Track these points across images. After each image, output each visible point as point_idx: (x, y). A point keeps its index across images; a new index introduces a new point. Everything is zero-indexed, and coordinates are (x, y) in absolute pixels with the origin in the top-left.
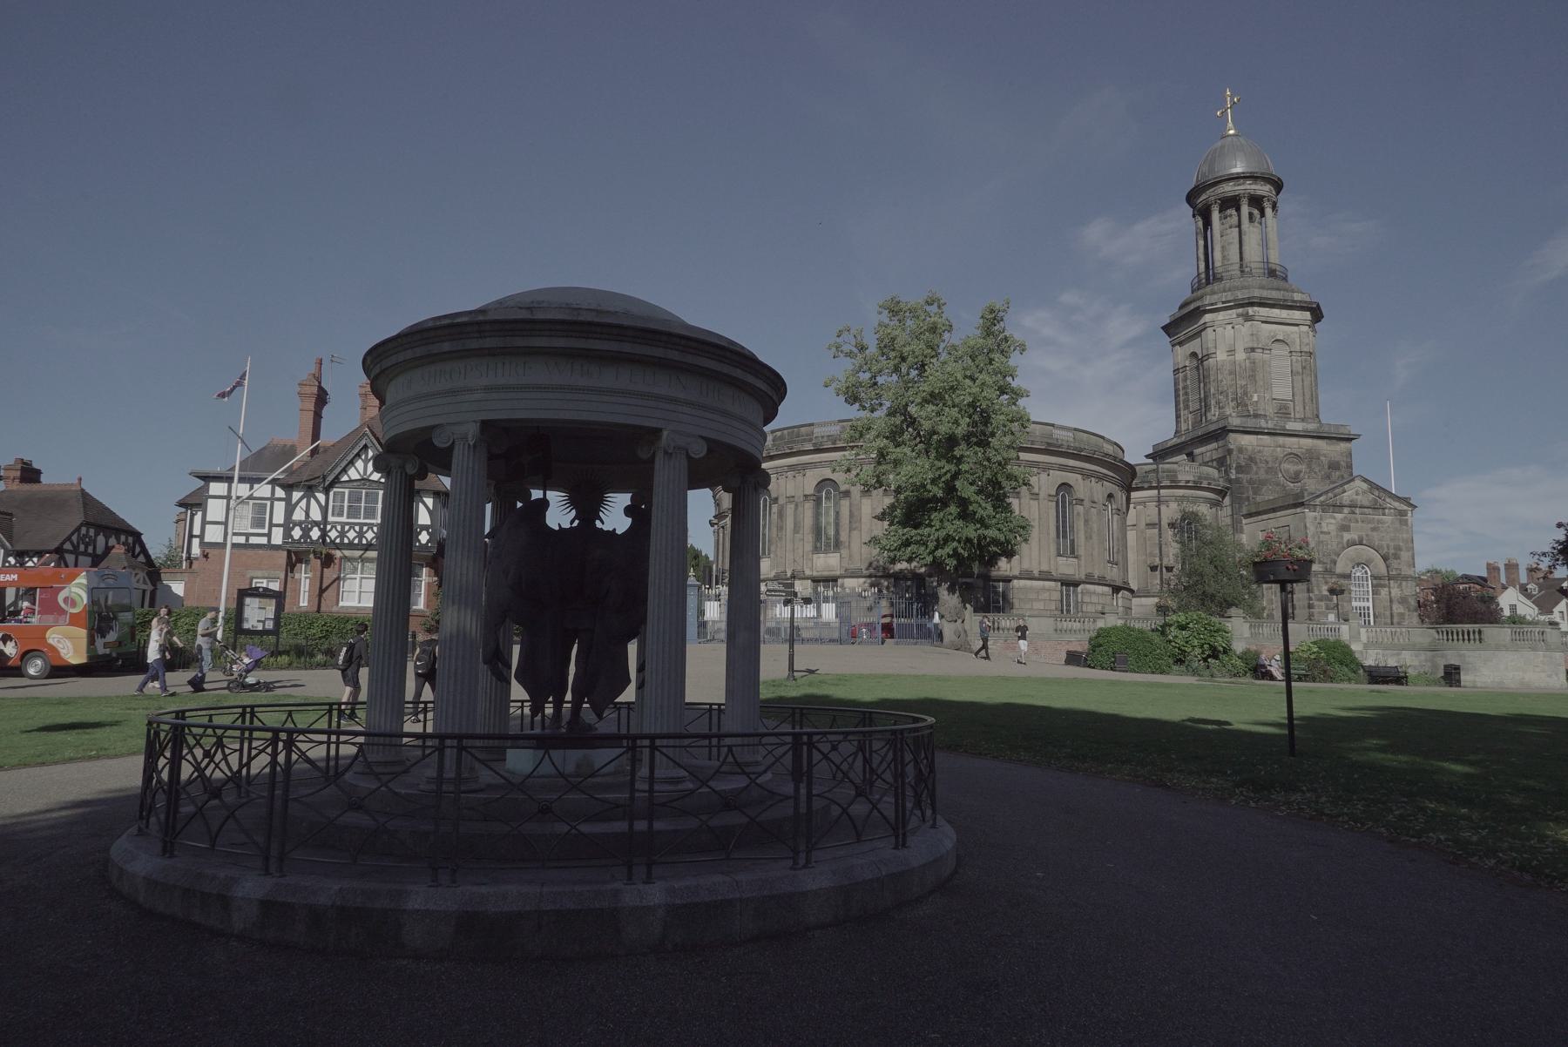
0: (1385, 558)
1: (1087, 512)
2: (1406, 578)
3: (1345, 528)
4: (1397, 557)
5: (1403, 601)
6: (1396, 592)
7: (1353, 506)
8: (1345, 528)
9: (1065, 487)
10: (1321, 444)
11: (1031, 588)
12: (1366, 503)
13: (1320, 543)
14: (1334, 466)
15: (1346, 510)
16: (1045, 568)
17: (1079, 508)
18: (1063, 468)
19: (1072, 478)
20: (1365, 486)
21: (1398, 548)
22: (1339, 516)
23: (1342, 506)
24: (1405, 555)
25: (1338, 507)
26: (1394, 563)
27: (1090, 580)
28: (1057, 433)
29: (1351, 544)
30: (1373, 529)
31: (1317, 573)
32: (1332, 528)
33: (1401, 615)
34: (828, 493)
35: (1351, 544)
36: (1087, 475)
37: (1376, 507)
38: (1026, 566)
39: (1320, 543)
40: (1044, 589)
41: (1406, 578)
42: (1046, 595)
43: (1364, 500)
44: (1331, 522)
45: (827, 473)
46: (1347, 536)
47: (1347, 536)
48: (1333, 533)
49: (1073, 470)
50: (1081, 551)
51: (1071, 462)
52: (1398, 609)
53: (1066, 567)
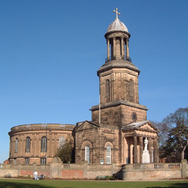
0: (92, 143)
1: (33, 142)
2: (97, 148)
3: (83, 136)
4: (95, 142)
5: (96, 155)
8: (83, 136)
9: (28, 137)
10: (113, 108)
12: (89, 128)
13: (78, 141)
14: (116, 113)
15: (84, 131)
16: (22, 155)
18: (27, 134)
19: (29, 135)
20: (88, 123)
21: (96, 140)
22: (82, 133)
23: (82, 130)
26: (94, 144)
27: (33, 157)
28: (27, 126)
30: (90, 135)
33: (95, 159)
34: (44, 139)
36: (33, 134)
39: (78, 141)
40: (21, 160)
41: (97, 148)
42: (21, 161)
43: (88, 127)
45: (45, 135)
46: (84, 138)
47: (84, 138)
48: (81, 138)
49: (29, 133)
50: (31, 151)
51: (29, 132)
52: (95, 157)
53: (27, 154)
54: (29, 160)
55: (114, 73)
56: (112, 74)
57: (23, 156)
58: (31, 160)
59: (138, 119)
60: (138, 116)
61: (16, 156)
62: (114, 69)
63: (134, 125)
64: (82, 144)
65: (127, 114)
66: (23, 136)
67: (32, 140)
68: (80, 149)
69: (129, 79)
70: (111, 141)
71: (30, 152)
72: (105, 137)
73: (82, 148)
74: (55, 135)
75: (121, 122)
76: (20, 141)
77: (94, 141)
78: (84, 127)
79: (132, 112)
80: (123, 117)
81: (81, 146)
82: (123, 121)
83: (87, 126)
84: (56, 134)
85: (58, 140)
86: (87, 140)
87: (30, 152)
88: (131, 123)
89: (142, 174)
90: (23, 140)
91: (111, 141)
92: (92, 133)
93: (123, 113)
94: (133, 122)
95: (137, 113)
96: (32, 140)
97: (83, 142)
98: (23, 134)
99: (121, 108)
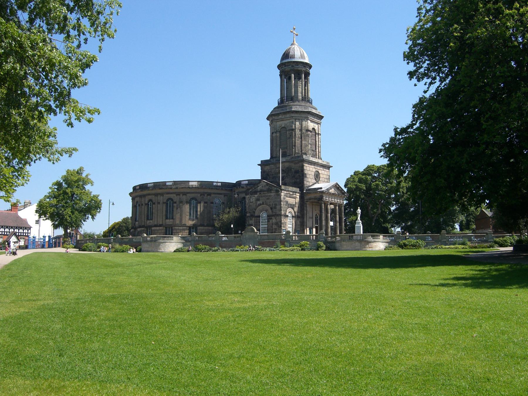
0: (271, 209)
3: (258, 200)
4: (275, 208)
6: (274, 221)
7: (261, 191)
8: (258, 200)
10: (293, 165)
11: (156, 230)
13: (250, 206)
14: (297, 172)
16: (161, 223)
17: (175, 205)
19: (171, 196)
21: (276, 205)
22: (256, 196)
24: (278, 207)
25: (255, 192)
26: (274, 210)
28: (168, 184)
29: (260, 205)
30: (267, 199)
31: (248, 216)
32: (254, 200)
33: (276, 229)
35: (260, 205)
37: (269, 190)
38: (156, 223)
39: (250, 206)
40: (160, 229)
44: (253, 199)
46: (258, 202)
47: (258, 202)
49: (171, 193)
52: (274, 227)
53: (169, 222)
54: (172, 230)
55: (294, 120)
56: (291, 121)
57: (162, 225)
58: (176, 230)
59: (321, 179)
60: (321, 176)
61: (150, 224)
62: (293, 115)
63: (321, 188)
64: (256, 210)
65: (309, 172)
66: (162, 197)
67: (175, 203)
68: (252, 216)
69: (310, 128)
70: (292, 207)
71: (173, 218)
72: (287, 202)
73: (256, 214)
74: (208, 197)
75: (303, 183)
76: (156, 203)
77: (274, 206)
78: (259, 188)
79: (314, 170)
80: (306, 177)
81: (254, 212)
82: (305, 182)
83: (263, 187)
84: (209, 194)
85: (212, 203)
86: (263, 204)
87: (173, 218)
88: (313, 184)
89: (359, 244)
90: (161, 202)
91: (292, 207)
92: (270, 196)
93: (306, 172)
94: (315, 183)
95: (320, 172)
96: (175, 203)
97: (257, 207)
98: (162, 194)
99: (303, 166)
